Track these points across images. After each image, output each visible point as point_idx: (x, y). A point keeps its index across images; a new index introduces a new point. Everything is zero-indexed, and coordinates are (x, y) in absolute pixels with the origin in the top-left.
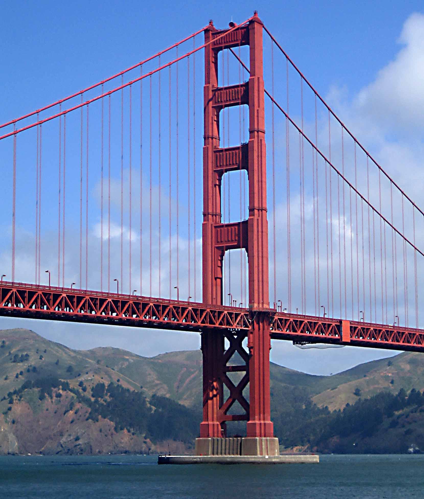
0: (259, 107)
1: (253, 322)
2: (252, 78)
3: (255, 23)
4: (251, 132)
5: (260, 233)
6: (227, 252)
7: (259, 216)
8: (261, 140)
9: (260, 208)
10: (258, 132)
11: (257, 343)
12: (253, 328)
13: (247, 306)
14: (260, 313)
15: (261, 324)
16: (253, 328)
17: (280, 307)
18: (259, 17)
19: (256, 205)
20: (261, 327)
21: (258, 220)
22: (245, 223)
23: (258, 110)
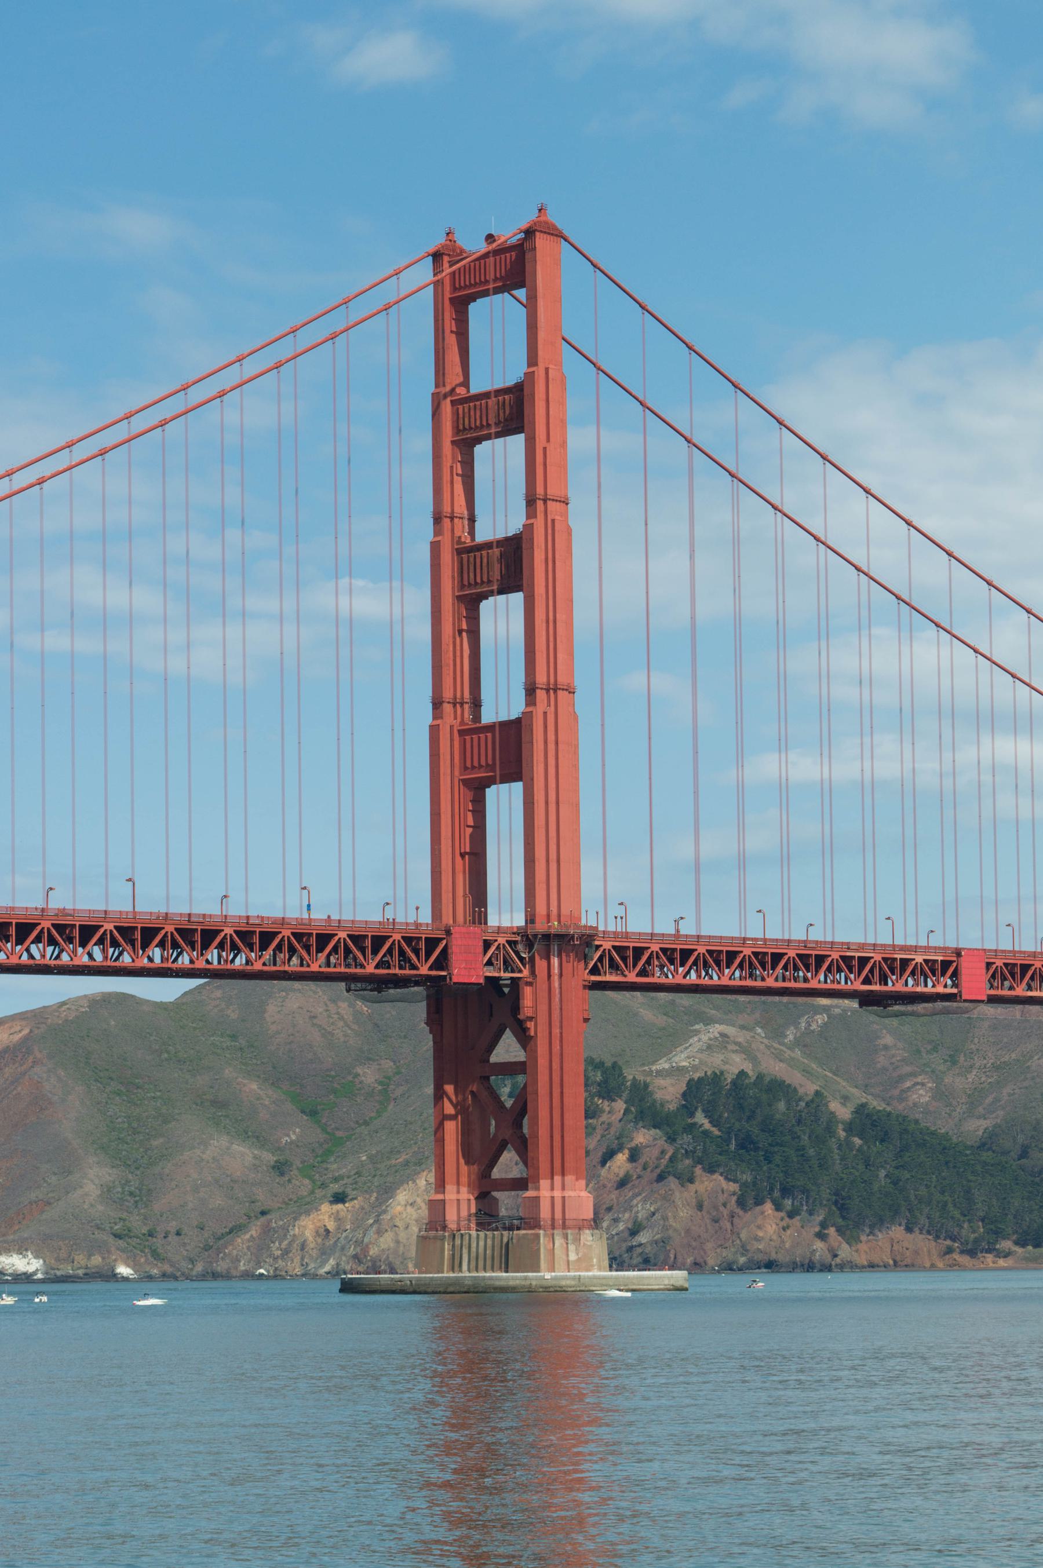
0: (548, 440)
1: (532, 960)
2: (531, 370)
3: (537, 234)
4: (531, 502)
5: (551, 746)
6: (491, 792)
7: (549, 705)
8: (553, 521)
9: (551, 686)
10: (545, 501)
11: (543, 1008)
12: (533, 972)
13: (519, 921)
14: (547, 937)
15: (555, 961)
16: (533, 972)
17: (622, 918)
18: (554, 217)
19: (541, 679)
20: (556, 970)
21: (545, 713)
22: (518, 721)
23: (545, 449)
